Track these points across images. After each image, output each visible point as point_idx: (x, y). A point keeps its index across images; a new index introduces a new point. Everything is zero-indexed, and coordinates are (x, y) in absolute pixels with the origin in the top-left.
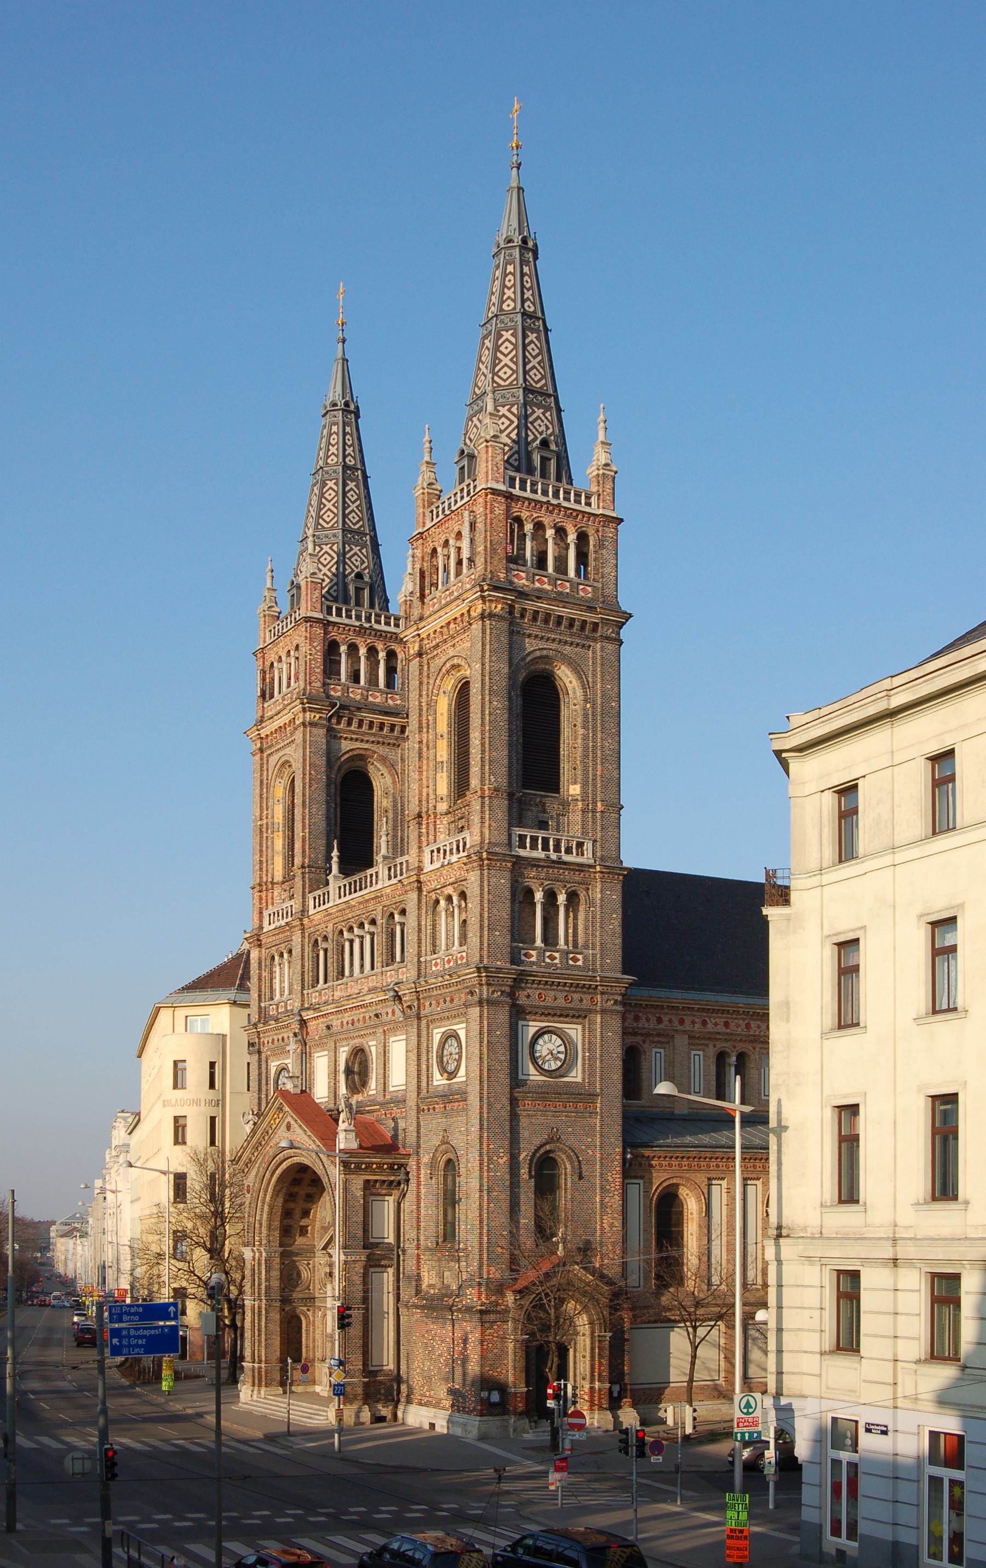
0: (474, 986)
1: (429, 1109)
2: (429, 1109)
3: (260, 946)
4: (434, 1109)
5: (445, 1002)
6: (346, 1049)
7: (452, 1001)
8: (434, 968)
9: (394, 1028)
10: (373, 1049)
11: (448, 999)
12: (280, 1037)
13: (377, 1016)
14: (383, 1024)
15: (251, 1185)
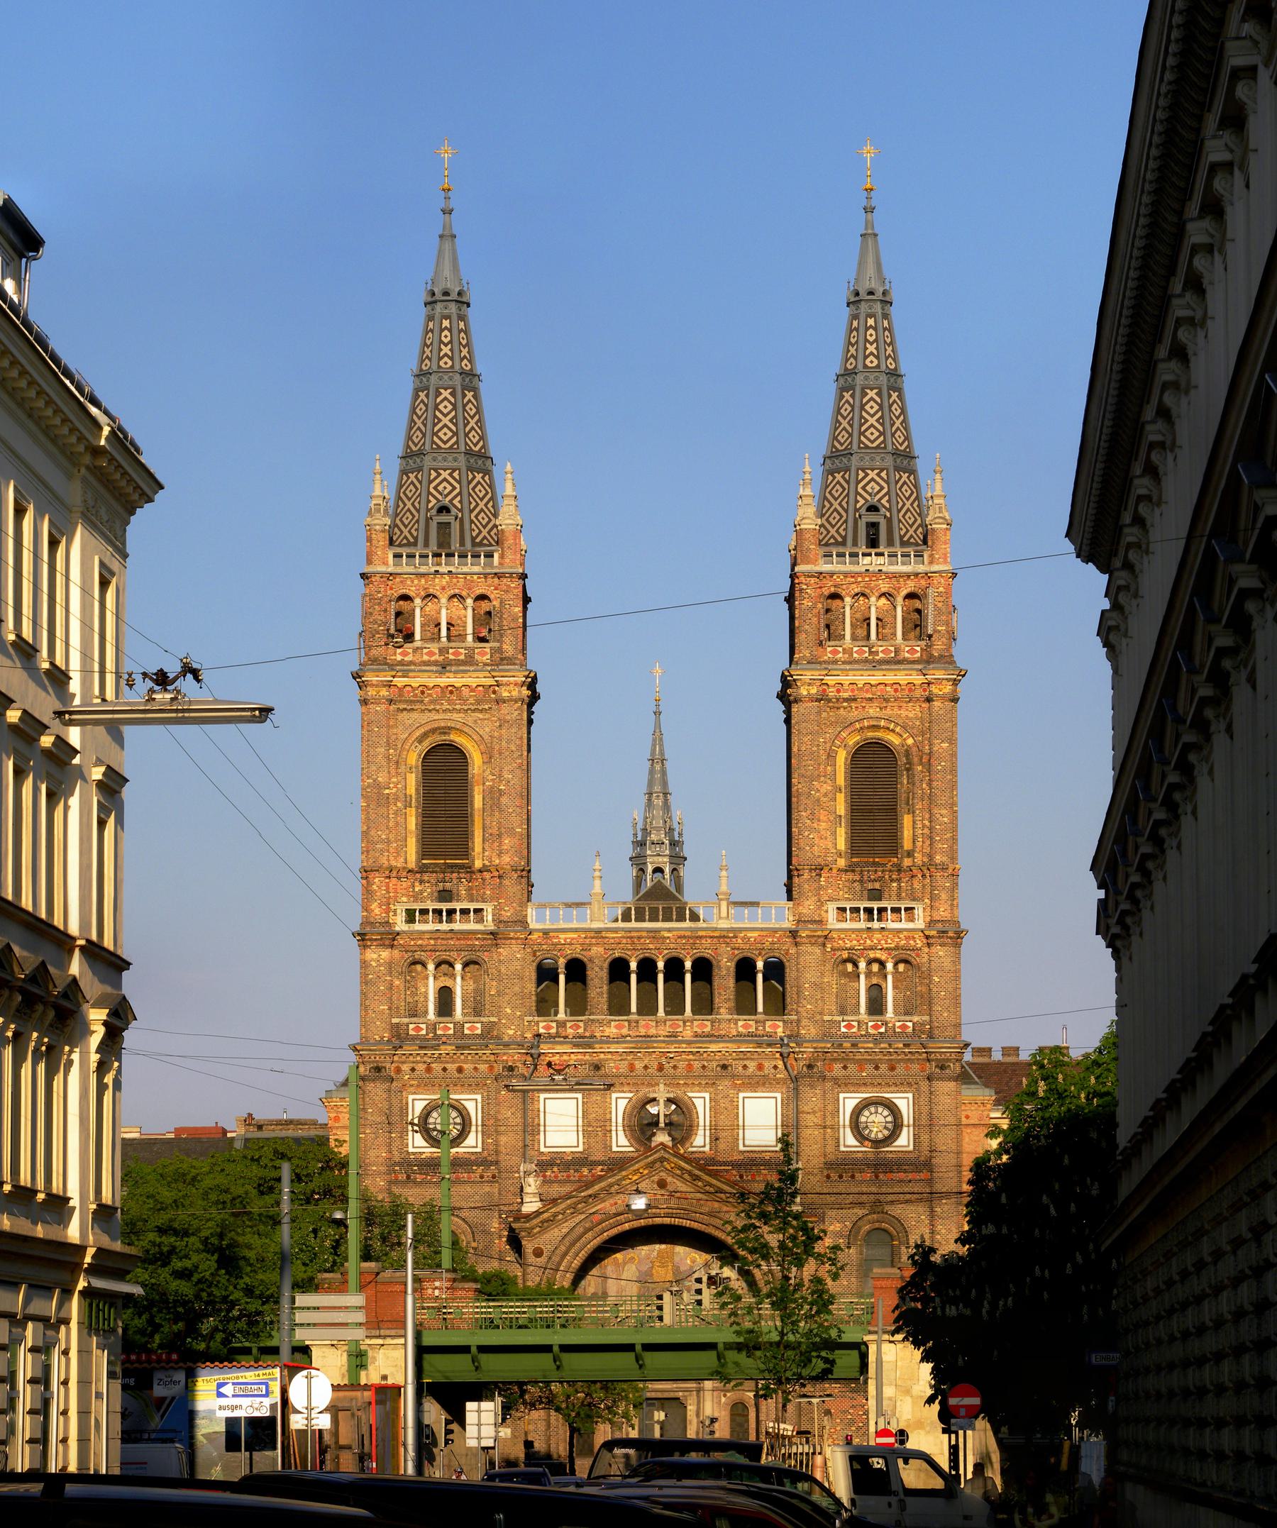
0: (948, 1060)
1: (841, 1177)
2: (841, 1177)
3: (392, 946)
4: (853, 1177)
5: (877, 1068)
6: (630, 1095)
7: (892, 1068)
8: (843, 1030)
9: (758, 1083)
10: (699, 1103)
11: (883, 1067)
12: (452, 1067)
13: (724, 1067)
14: (733, 1076)
15: (547, 1249)
